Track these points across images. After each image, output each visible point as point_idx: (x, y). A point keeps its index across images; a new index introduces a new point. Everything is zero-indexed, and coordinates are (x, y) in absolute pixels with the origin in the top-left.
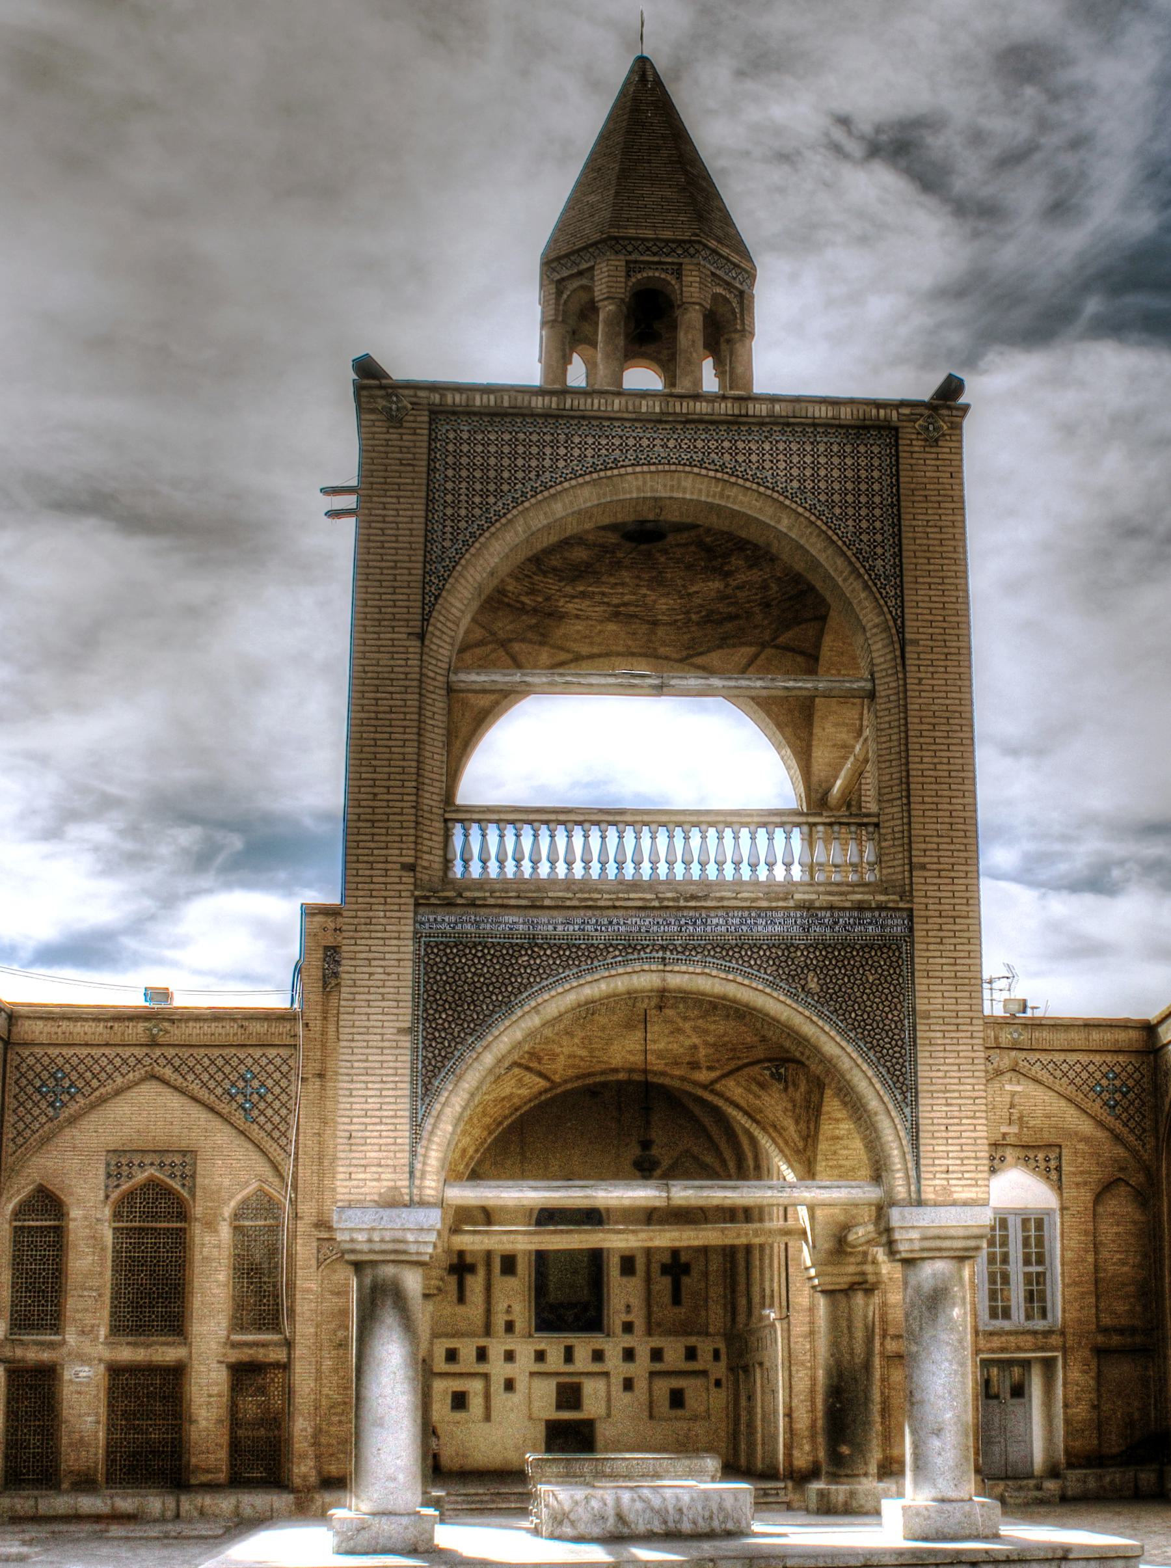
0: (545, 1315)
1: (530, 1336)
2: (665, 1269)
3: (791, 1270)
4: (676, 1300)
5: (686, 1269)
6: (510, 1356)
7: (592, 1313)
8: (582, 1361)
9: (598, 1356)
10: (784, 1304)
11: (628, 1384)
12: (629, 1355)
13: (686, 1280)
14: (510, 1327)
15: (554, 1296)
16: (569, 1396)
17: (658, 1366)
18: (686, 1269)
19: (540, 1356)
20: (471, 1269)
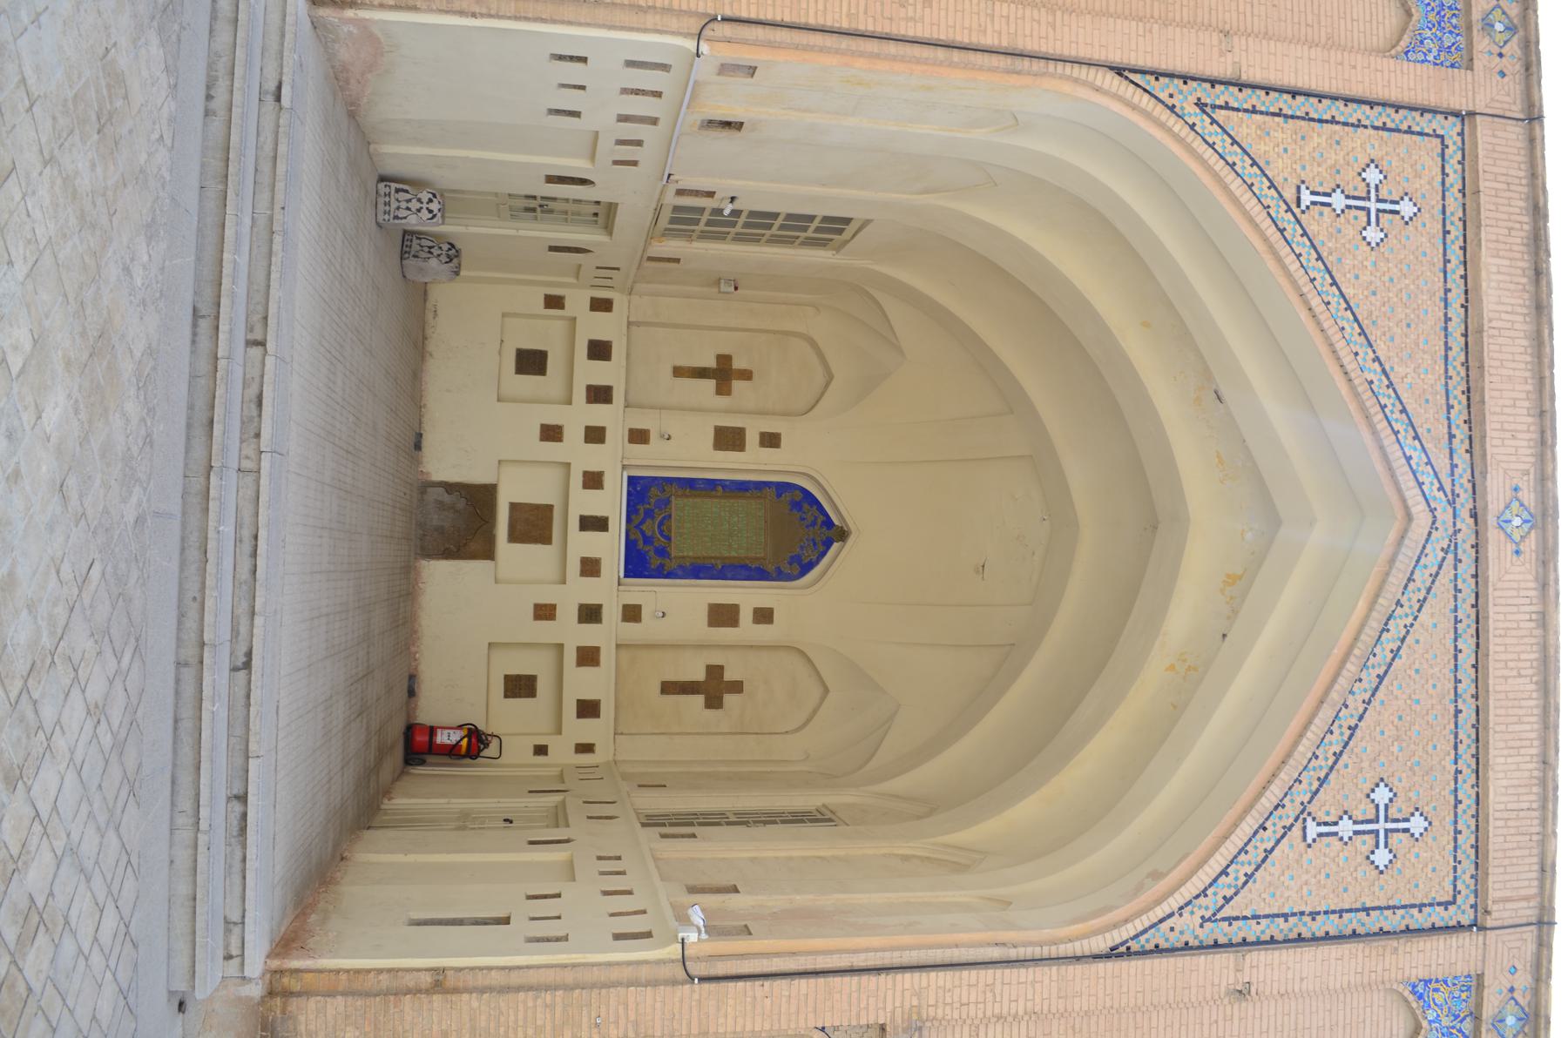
0: (654, 491)
1: (624, 467)
2: (715, 671)
3: (803, 983)
4: (668, 688)
5: (714, 702)
6: (595, 435)
7: (655, 561)
8: (584, 544)
9: (590, 567)
10: (721, 969)
11: (545, 612)
12: (590, 614)
13: (699, 699)
14: (639, 436)
15: (681, 507)
16: (534, 524)
17: (570, 657)
18: (714, 702)
19: (593, 480)
20: (723, 389)
